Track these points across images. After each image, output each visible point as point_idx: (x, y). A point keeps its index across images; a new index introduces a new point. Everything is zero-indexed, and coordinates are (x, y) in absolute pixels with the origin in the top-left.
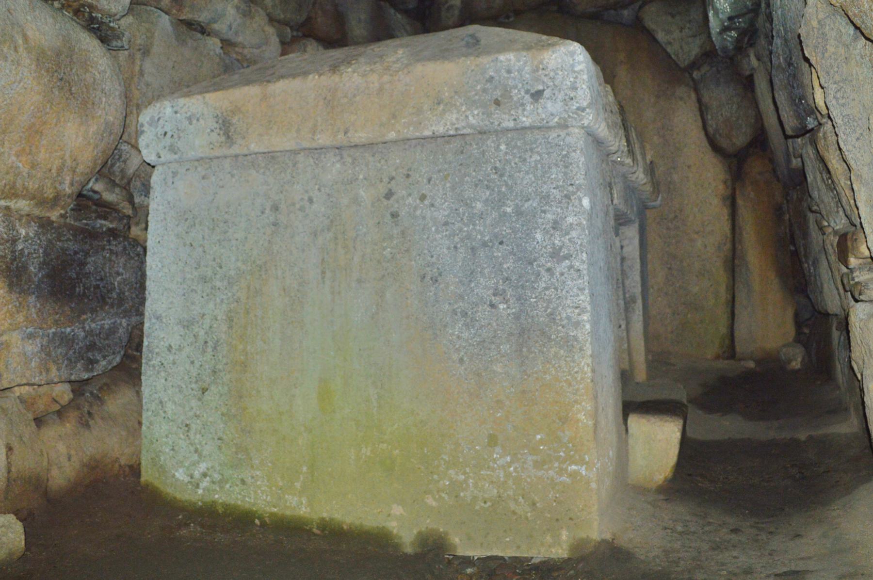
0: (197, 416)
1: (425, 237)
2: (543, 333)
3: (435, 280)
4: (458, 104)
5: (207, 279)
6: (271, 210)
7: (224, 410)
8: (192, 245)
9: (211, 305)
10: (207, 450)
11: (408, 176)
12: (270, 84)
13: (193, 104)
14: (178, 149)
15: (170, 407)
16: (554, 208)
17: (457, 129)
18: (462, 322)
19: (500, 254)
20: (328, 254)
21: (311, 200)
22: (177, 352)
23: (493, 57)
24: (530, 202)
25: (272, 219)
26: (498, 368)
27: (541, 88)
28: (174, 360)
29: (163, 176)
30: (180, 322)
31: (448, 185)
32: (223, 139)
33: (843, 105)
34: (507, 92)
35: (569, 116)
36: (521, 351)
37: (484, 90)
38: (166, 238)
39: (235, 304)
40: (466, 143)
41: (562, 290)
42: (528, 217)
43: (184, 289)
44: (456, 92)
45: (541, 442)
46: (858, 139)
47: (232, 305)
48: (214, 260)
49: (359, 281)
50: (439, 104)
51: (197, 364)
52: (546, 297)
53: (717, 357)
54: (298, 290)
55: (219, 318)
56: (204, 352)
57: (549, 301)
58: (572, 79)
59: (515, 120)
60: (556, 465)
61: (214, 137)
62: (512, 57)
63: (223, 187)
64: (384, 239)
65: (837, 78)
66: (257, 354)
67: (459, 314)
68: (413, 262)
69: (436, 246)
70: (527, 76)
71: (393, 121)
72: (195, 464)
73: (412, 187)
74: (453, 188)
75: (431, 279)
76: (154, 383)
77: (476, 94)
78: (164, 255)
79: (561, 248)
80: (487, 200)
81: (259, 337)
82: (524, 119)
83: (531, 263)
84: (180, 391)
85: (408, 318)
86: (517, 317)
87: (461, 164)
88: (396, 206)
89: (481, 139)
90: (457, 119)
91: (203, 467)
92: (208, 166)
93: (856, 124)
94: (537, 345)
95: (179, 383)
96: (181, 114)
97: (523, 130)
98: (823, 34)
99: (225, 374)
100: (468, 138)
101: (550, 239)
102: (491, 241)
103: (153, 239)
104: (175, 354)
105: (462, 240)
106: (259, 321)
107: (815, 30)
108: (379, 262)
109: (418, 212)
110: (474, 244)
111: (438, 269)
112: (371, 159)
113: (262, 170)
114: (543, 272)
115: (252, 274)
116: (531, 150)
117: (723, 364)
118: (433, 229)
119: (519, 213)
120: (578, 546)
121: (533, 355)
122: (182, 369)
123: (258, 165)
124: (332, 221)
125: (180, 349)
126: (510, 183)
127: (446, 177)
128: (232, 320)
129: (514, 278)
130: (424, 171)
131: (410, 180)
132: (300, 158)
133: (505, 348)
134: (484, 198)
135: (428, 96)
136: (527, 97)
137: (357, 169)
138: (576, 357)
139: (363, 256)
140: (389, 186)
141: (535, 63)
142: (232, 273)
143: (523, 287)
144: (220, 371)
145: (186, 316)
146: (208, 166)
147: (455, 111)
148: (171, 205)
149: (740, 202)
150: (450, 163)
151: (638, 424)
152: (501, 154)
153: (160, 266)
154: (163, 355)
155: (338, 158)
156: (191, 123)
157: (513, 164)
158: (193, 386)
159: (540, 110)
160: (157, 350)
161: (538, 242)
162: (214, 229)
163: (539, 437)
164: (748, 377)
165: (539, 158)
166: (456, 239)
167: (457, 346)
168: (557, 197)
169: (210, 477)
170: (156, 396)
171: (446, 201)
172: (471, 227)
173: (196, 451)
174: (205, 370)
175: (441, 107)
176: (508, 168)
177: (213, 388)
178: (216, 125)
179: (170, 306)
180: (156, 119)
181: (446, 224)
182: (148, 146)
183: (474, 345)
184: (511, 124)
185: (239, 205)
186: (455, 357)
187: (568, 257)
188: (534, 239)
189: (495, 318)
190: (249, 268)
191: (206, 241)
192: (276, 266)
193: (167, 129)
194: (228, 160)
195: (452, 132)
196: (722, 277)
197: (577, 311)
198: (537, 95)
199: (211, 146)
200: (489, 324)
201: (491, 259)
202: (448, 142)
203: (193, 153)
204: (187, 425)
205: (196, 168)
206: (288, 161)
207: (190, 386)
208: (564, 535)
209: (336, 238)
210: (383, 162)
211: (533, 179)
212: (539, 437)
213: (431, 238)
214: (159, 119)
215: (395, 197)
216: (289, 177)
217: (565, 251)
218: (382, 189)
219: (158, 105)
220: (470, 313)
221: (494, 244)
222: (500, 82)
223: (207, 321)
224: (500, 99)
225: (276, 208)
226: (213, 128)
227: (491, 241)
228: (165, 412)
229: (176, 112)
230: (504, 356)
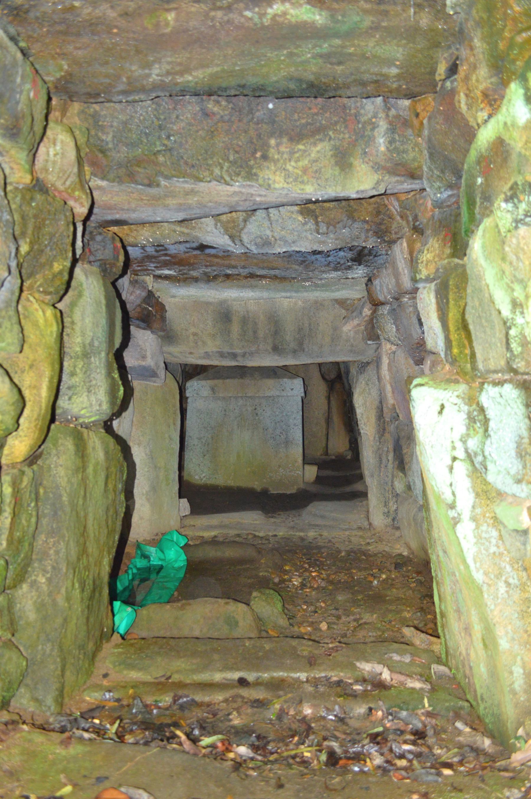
10: (205, 471)
15: (194, 460)
30: (197, 438)
34: (285, 388)
53: (322, 455)
91: (204, 475)
97: (288, 396)
117: (323, 457)
119: (287, 415)
120: (298, 489)
149: (332, 398)
151: (307, 467)
164: (333, 461)
196: (324, 425)
198: (292, 389)
208: (295, 487)
218: (254, 408)
225: (225, 411)
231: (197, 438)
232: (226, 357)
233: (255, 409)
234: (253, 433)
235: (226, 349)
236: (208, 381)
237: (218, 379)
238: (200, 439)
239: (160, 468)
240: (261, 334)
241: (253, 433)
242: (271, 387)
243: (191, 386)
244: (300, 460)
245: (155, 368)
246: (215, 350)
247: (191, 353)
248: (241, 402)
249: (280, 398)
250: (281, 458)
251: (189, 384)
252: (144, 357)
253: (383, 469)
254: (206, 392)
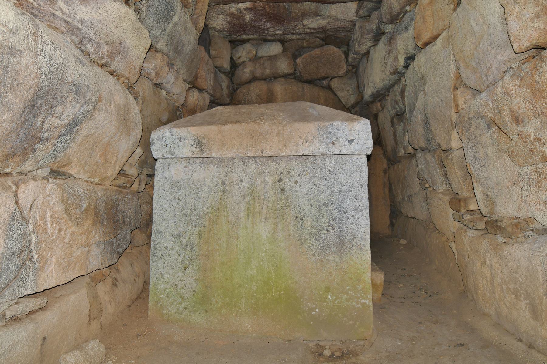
0: (182, 280)
1: (297, 200)
2: (350, 243)
3: (302, 219)
4: (315, 142)
5: (188, 215)
6: (221, 184)
7: (197, 277)
8: (179, 199)
9: (190, 228)
11: (289, 172)
12: (222, 126)
13: (181, 131)
14: (174, 153)
15: (166, 276)
16: (355, 190)
17: (313, 153)
18: (314, 238)
19: (331, 209)
20: (250, 205)
21: (241, 181)
22: (171, 250)
23: (331, 123)
24: (345, 187)
25: (222, 188)
26: (330, 258)
27: (353, 138)
28: (169, 253)
29: (163, 165)
30: (172, 235)
31: (308, 177)
32: (199, 150)
33: (475, 153)
35: (362, 150)
36: (340, 251)
37: (327, 138)
38: (164, 195)
39: (203, 228)
40: (316, 159)
41: (359, 225)
42: (344, 193)
43: (175, 220)
44: (314, 137)
45: (349, 290)
46: (481, 167)
47: (201, 228)
48: (192, 206)
49: (266, 219)
50: (306, 142)
51: (182, 255)
52: (351, 228)
54: (235, 222)
55: (194, 234)
56: (186, 250)
57: (353, 230)
58: (366, 136)
59: (340, 151)
60: (356, 300)
61: (193, 148)
62: (340, 124)
63: (196, 172)
64: (278, 200)
65: (474, 141)
66: (214, 251)
67: (313, 234)
68: (292, 211)
69: (302, 204)
70: (347, 133)
71: (285, 148)
72: (180, 303)
73: (291, 177)
74: (310, 179)
75: (300, 219)
76: (157, 265)
77: (323, 139)
78: (163, 203)
79: (358, 207)
80: (326, 185)
81: (215, 243)
82: (345, 151)
83: (345, 213)
84: (172, 268)
85: (289, 235)
86: (339, 236)
87: (314, 169)
88: (284, 185)
89: (323, 158)
90: (314, 149)
91: (184, 305)
92: (187, 161)
93: (481, 161)
94: (347, 248)
95: (172, 265)
96: (175, 136)
98: (469, 123)
99: (197, 261)
100: (317, 157)
101: (353, 203)
102: (327, 203)
103: (157, 195)
104: (170, 250)
105: (314, 202)
106: (215, 236)
107: (466, 121)
108: (275, 210)
109: (294, 189)
110: (319, 204)
111: (303, 214)
112: (271, 164)
113: (216, 165)
114: (350, 217)
115: (211, 214)
116: (345, 164)
118: (301, 196)
121: (346, 252)
122: (173, 258)
123: (215, 163)
124: (252, 191)
125: (172, 248)
126: (336, 178)
127: (307, 174)
128: (201, 235)
129: (337, 219)
130: (297, 170)
131: (290, 174)
132: (236, 161)
133: (333, 249)
134: (324, 184)
135: (301, 138)
136: (347, 142)
137: (264, 167)
138: (364, 254)
139: (268, 207)
140: (280, 176)
141: (350, 127)
142: (201, 213)
143: (341, 223)
144: (194, 259)
145: (176, 233)
146: (187, 161)
147: (314, 146)
148: (167, 179)
150: (309, 167)
152: (332, 165)
153: (161, 208)
154: (163, 251)
155: (254, 162)
156: (180, 141)
157: (337, 170)
158: (180, 266)
159: (352, 148)
160: (159, 249)
161: (348, 204)
162: (191, 192)
163: (348, 288)
165: (348, 168)
166: (312, 201)
167: (312, 249)
168: (357, 185)
169: (188, 309)
170: (159, 271)
171: (307, 184)
172: (318, 196)
173: (181, 297)
174: (186, 258)
175: (307, 143)
176: (335, 171)
177: (190, 267)
178: (194, 143)
179: (167, 227)
180: (161, 137)
181: (307, 194)
182: (157, 150)
183: (319, 248)
184: (338, 153)
185: (205, 181)
186: (311, 253)
187: (360, 211)
188: (347, 202)
189: (329, 236)
190: (210, 211)
191: (187, 197)
192: (224, 210)
193: (167, 143)
194: (198, 159)
195: (310, 154)
197: (365, 234)
198: (351, 141)
199: (192, 153)
200: (326, 239)
201: (327, 211)
202: (307, 158)
203: (182, 156)
204: (176, 285)
205: (181, 162)
206: (230, 162)
207: (177, 266)
209: (254, 199)
210: (277, 165)
211: (346, 176)
212: (348, 288)
213: (300, 201)
214: (163, 138)
215: (283, 181)
216: (230, 169)
217: (360, 209)
218: (277, 177)
219: (162, 131)
220: (318, 234)
221: (328, 204)
222: (334, 134)
223: (188, 235)
224: (334, 142)
225: (224, 183)
226: (193, 144)
227: (327, 203)
228: (163, 279)
229: (172, 135)
230: (333, 253)
231: (172, 235)
234: (276, 224)
237: (210, 124)
238: (177, 237)
241: (276, 224)
242: (310, 138)
243: (161, 139)
248: (252, 167)
249: (327, 159)
250: (331, 273)
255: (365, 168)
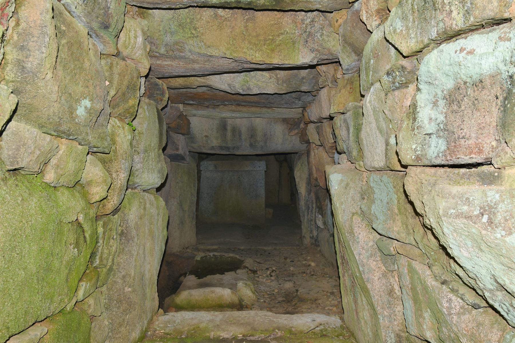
198: (260, 167)
225: (222, 178)
232: (223, 149)
233: (239, 177)
235: (224, 145)
236: (213, 162)
239: (186, 211)
240: (243, 137)
244: (264, 206)
245: (184, 155)
246: (217, 145)
247: (204, 147)
251: (202, 163)
252: (177, 149)
253: (310, 213)
254: (212, 168)
255: (264, 174)
